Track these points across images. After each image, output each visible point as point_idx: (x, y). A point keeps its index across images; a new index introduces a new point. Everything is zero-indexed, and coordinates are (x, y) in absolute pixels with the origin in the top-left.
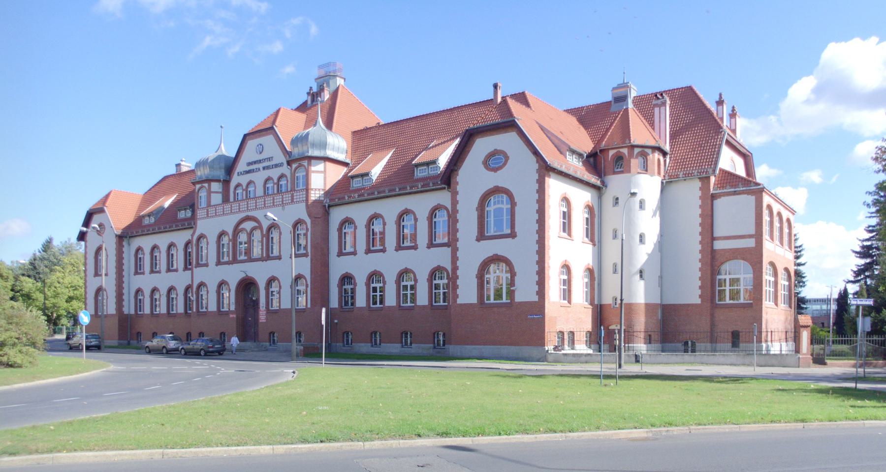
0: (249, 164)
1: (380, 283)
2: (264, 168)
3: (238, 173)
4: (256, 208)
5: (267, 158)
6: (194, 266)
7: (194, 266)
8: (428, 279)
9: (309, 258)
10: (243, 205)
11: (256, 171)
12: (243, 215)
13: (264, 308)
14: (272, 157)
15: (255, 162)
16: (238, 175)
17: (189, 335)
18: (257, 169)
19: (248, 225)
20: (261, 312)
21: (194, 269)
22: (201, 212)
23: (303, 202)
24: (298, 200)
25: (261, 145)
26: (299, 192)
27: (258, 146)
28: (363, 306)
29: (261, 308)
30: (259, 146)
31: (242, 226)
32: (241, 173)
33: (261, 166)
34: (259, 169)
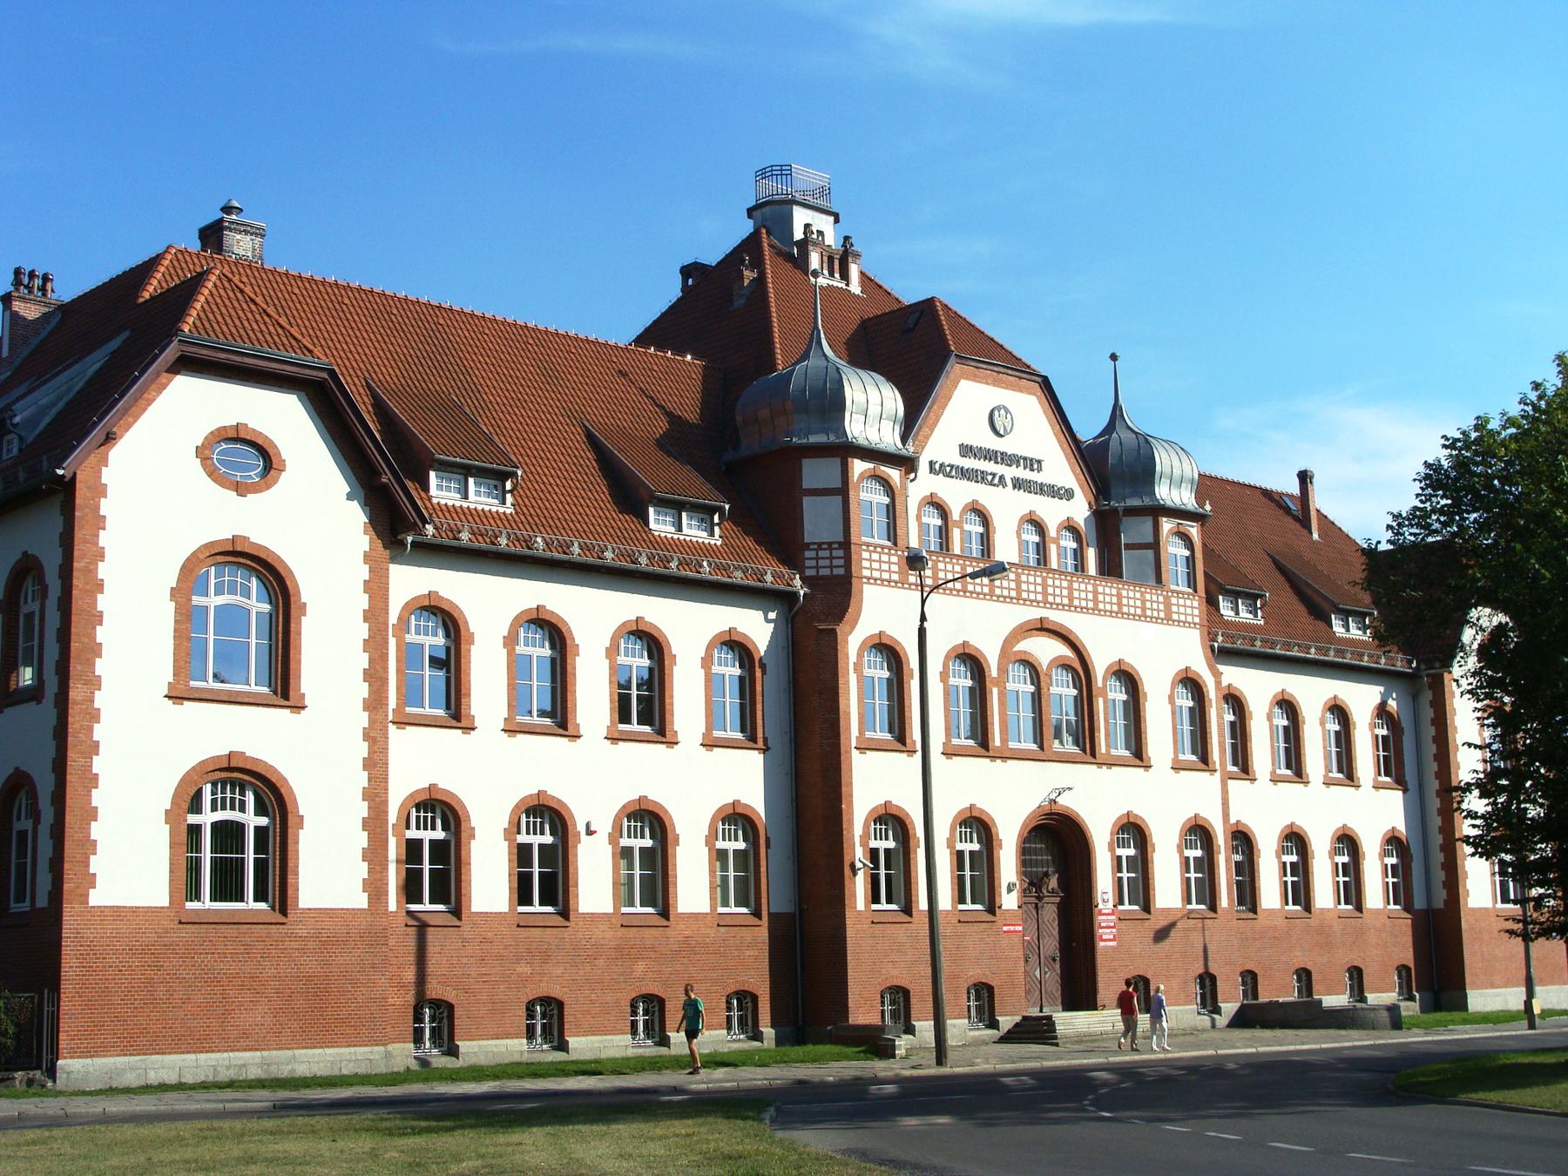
0: (966, 450)
1: (1196, 848)
2: (1018, 484)
3: (931, 463)
4: (1070, 607)
5: (1025, 459)
6: (854, 744)
7: (854, 744)
8: (473, 836)
9: (1218, 772)
10: (1032, 582)
11: (991, 484)
12: (1034, 613)
13: (1110, 905)
14: (1039, 462)
15: (990, 455)
16: (932, 470)
17: (1356, 974)
18: (994, 475)
19: (1046, 650)
20: (1100, 918)
21: (855, 753)
22: (875, 556)
23: (1195, 627)
24: (1182, 618)
25: (1007, 411)
26: (1178, 597)
27: (998, 408)
28: (503, 911)
29: (1101, 906)
30: (1002, 412)
31: (1017, 648)
32: (941, 465)
33: (1010, 472)
34: (1002, 477)
